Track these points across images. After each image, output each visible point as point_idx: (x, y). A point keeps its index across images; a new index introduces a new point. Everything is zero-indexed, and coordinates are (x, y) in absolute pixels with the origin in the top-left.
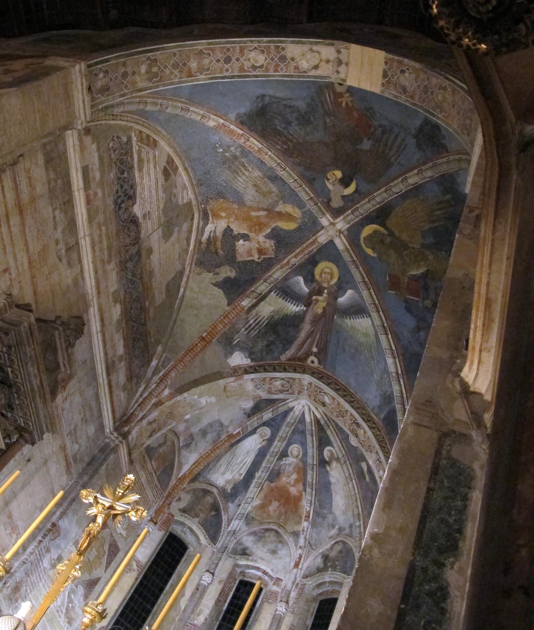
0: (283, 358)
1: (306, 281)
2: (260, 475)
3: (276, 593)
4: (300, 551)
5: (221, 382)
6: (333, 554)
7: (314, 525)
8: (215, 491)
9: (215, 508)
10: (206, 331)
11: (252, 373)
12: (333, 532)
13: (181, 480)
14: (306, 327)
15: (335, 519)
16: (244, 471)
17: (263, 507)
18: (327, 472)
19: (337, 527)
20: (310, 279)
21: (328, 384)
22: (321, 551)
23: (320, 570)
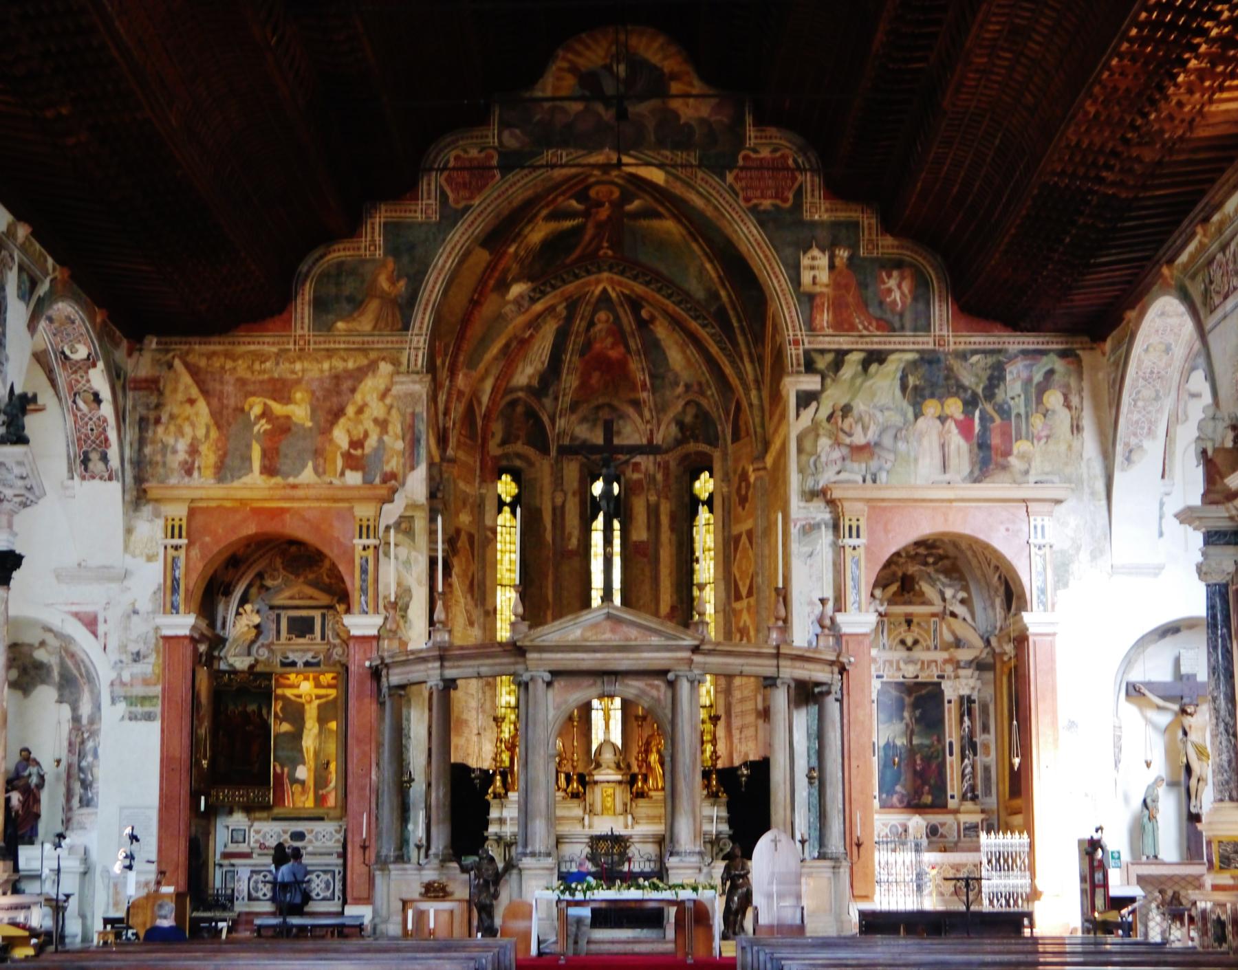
0: (568, 261)
1: (579, 202)
2: (570, 358)
3: (639, 482)
4: (649, 427)
5: (510, 327)
6: (688, 419)
7: (654, 390)
8: (520, 394)
9: (532, 415)
10: (475, 291)
11: (539, 299)
12: (680, 389)
13: (487, 417)
14: (590, 231)
15: (676, 376)
16: (545, 357)
17: (584, 385)
18: (652, 331)
19: (682, 384)
20: (582, 196)
21: (635, 278)
22: (672, 415)
23: (679, 442)
